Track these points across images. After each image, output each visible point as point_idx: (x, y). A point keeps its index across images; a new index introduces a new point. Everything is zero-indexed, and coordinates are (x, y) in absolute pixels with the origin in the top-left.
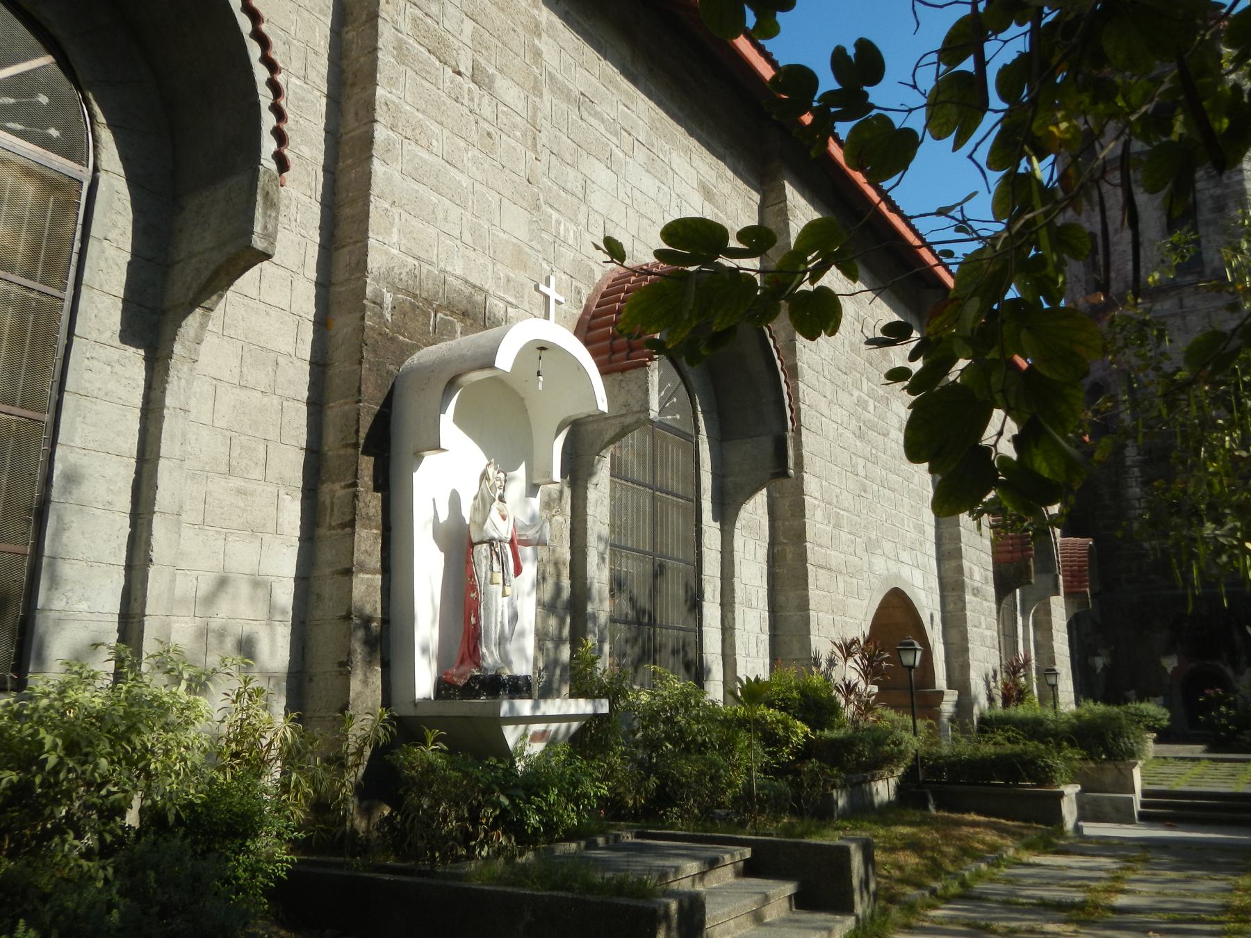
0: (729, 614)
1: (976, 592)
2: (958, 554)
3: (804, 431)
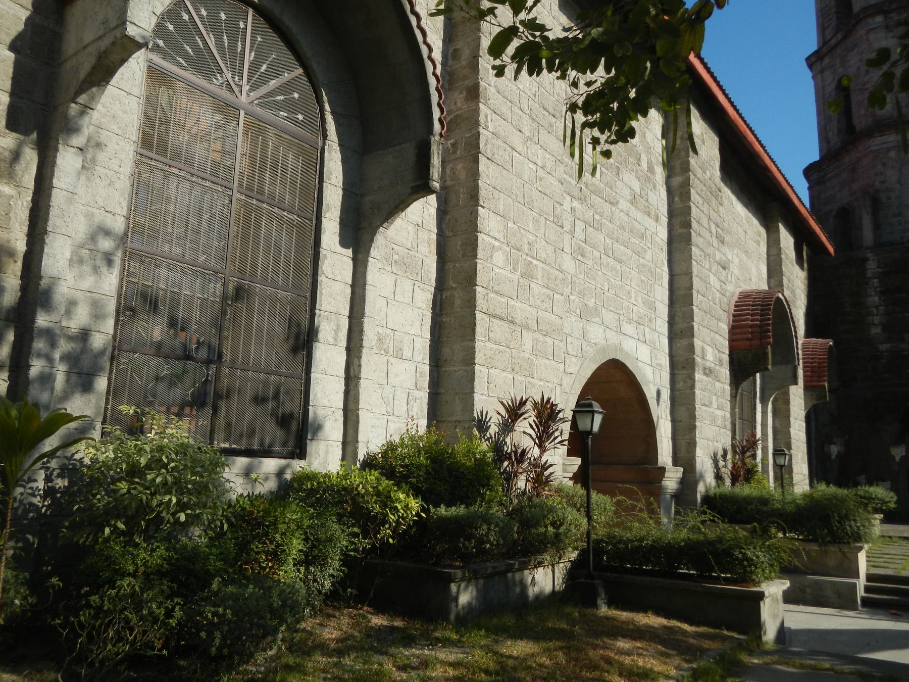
0: (356, 361)
1: (708, 372)
2: (689, 332)
3: (482, 160)
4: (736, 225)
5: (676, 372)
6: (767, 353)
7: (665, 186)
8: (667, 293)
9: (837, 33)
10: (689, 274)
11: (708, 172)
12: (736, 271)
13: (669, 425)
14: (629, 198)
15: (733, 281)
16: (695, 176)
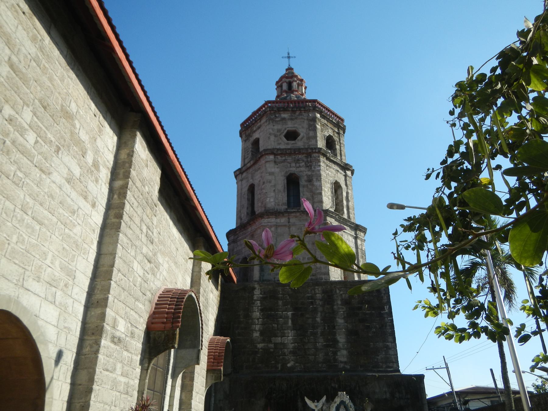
1: (117, 341)
2: (104, 303)
4: (170, 241)
5: (86, 337)
6: (175, 334)
7: (108, 185)
8: (91, 267)
9: (251, 161)
10: (113, 255)
11: (146, 187)
12: (165, 273)
13: (66, 389)
14: (65, 176)
15: (161, 279)
16: (134, 184)
